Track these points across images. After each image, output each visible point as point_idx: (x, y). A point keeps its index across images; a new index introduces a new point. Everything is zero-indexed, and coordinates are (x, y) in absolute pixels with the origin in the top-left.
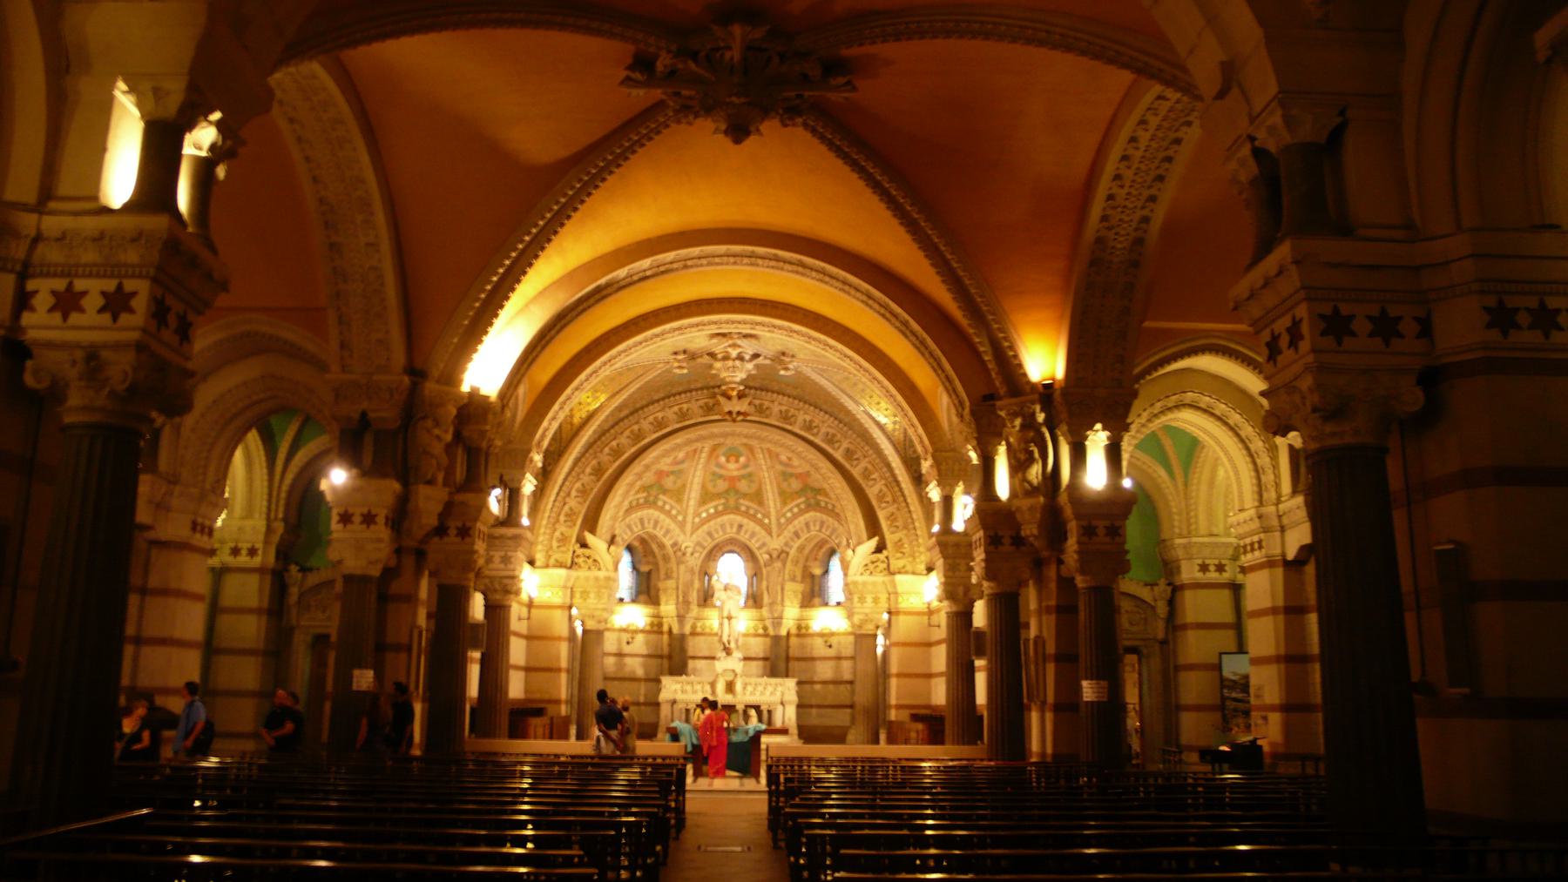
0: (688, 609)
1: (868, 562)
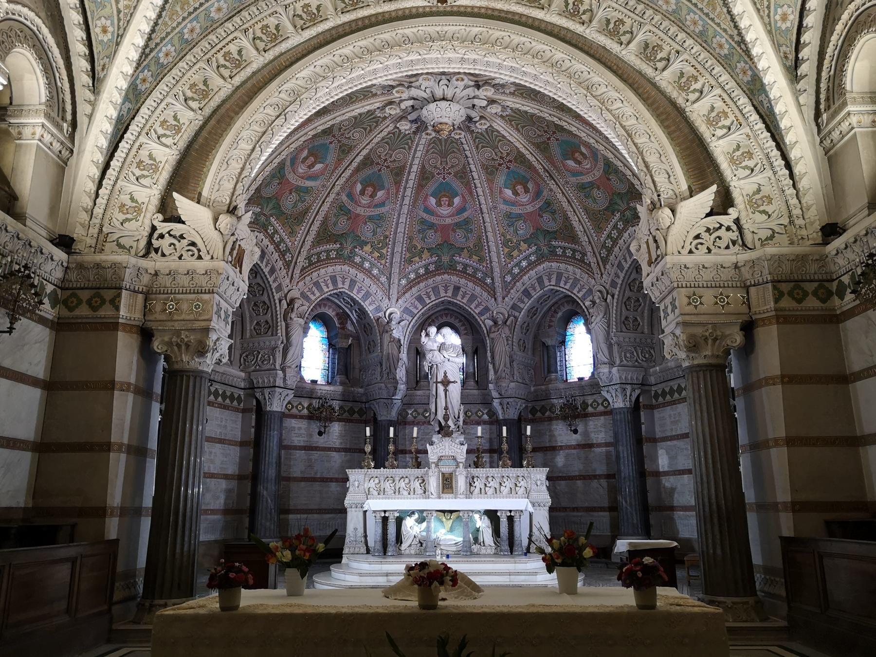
0: (396, 388)
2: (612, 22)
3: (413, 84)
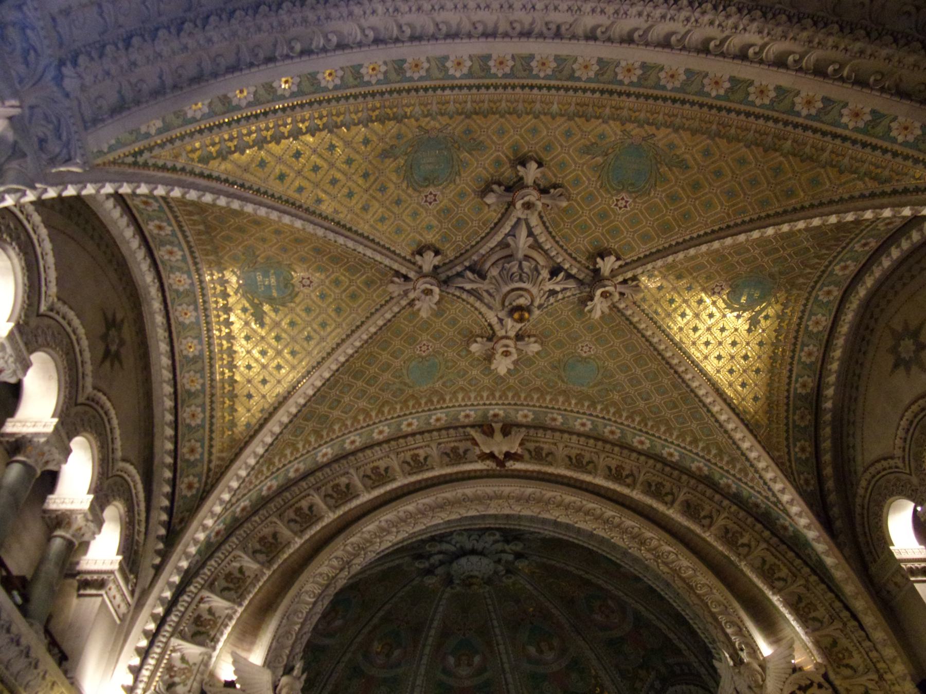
1: (795, 688)
2: (653, 484)
3: (445, 539)
